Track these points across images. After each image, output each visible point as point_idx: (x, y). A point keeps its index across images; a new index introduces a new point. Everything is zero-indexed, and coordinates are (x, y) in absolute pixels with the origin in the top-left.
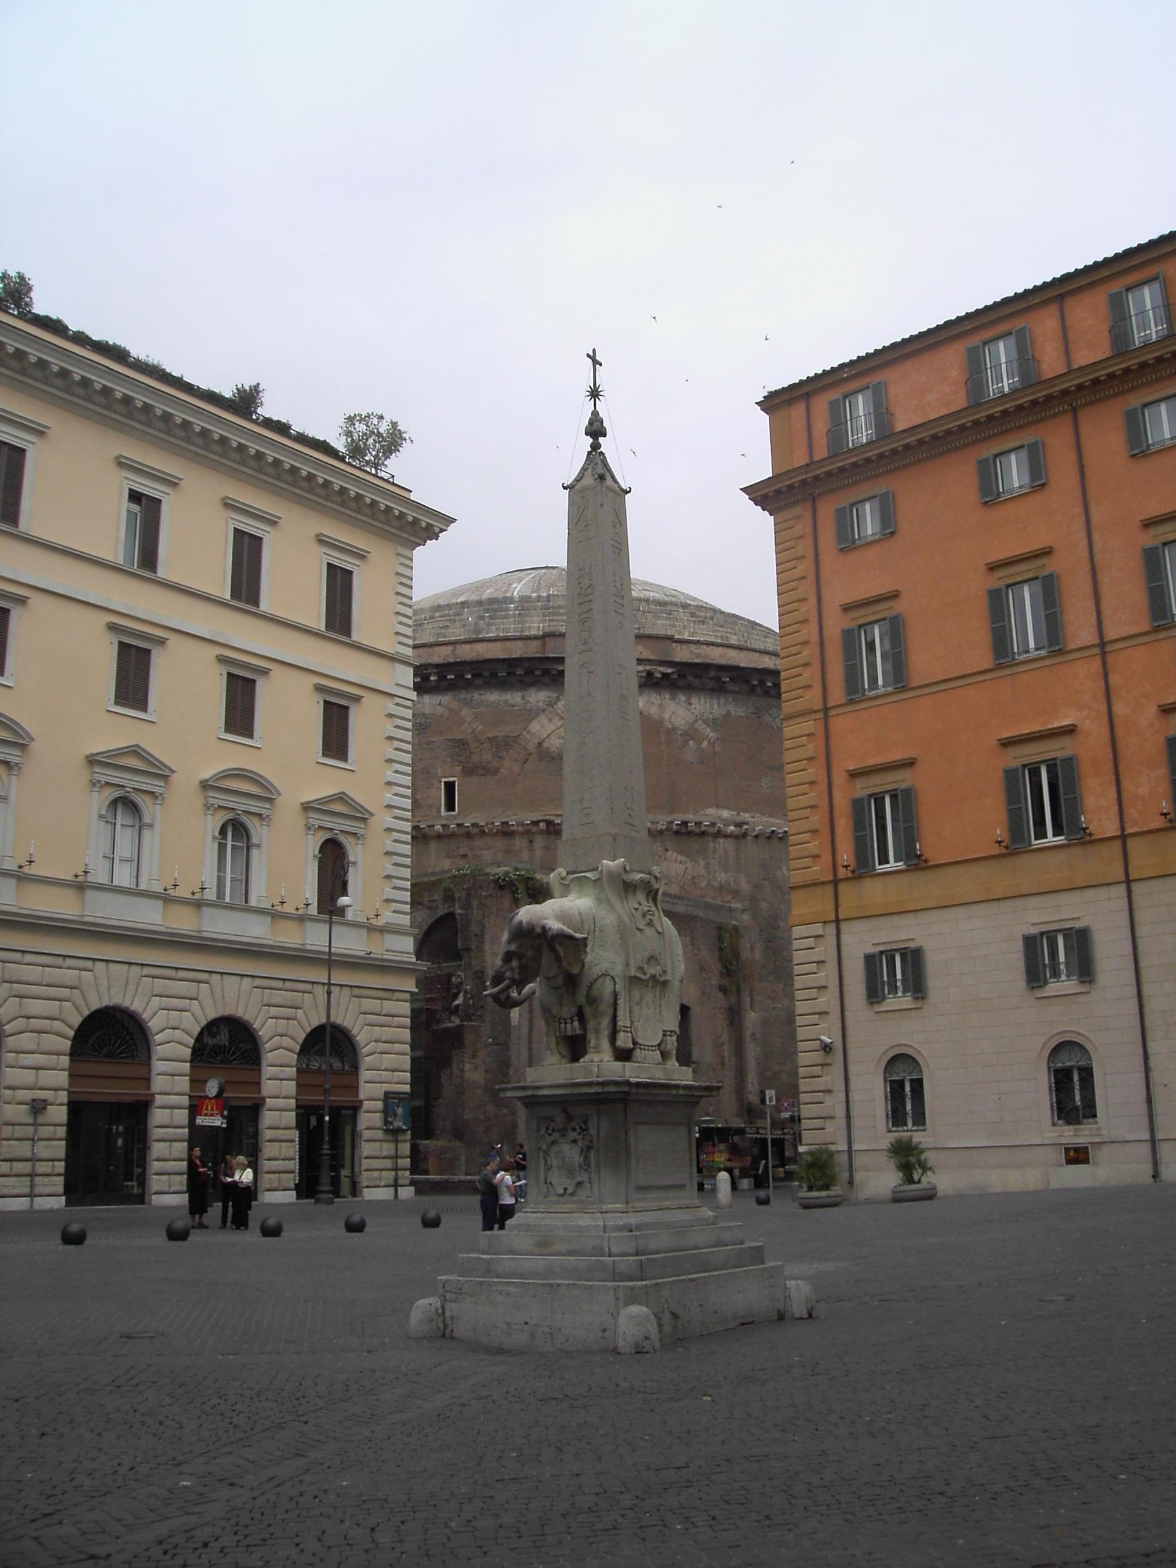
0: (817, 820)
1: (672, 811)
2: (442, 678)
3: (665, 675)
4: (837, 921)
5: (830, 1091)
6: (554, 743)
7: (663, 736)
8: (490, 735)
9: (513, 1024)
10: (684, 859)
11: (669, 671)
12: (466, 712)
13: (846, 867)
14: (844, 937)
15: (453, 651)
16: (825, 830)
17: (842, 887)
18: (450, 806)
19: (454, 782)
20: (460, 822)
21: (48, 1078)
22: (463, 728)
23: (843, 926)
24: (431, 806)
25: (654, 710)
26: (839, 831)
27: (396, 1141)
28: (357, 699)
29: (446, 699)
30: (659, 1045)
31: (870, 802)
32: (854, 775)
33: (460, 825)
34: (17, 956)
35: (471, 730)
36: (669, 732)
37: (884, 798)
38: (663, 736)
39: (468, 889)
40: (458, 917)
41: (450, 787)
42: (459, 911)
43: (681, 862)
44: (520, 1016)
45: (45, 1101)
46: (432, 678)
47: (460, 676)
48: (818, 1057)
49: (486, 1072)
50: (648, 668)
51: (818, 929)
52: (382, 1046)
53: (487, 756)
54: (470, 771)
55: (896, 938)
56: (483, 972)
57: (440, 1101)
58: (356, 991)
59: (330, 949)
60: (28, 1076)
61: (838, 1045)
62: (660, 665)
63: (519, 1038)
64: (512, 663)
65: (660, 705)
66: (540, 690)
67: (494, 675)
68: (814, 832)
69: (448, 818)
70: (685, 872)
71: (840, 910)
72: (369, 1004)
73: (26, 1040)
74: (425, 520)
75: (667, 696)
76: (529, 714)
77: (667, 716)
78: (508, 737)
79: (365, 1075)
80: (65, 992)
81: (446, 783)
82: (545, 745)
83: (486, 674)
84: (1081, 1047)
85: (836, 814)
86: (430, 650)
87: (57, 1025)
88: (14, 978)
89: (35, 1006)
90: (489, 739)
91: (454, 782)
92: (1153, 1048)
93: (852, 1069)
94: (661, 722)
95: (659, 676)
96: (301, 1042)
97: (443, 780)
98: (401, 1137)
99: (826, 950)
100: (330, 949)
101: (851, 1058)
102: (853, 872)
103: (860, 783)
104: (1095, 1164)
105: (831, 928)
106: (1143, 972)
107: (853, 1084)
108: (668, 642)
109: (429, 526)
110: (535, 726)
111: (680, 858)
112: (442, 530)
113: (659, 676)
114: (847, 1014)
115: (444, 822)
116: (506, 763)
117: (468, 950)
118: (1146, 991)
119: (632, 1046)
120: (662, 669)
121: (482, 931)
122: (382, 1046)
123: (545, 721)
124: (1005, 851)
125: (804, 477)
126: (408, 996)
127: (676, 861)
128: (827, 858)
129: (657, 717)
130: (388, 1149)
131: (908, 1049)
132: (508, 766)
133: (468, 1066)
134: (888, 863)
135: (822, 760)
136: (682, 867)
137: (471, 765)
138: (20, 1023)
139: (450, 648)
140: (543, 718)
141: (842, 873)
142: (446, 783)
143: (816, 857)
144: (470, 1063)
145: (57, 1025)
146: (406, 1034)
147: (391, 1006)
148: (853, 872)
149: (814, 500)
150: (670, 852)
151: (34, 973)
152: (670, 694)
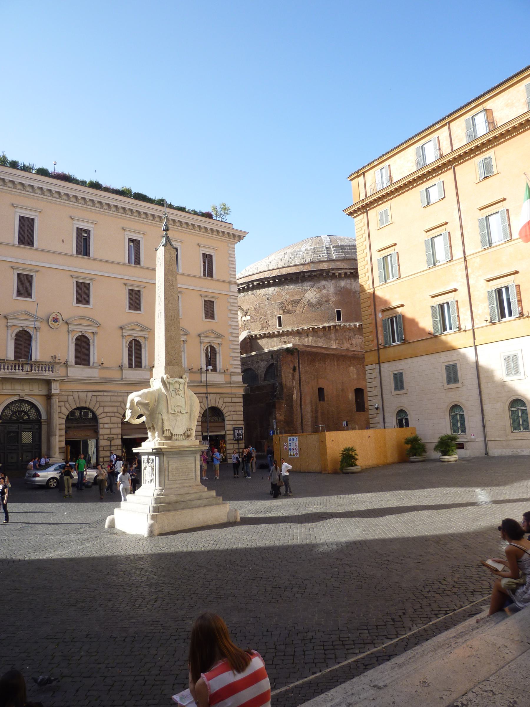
0: (372, 328)
1: (356, 321)
2: (274, 281)
3: (351, 273)
4: (379, 363)
5: (379, 423)
6: (314, 301)
7: (352, 295)
8: (291, 300)
9: (294, 399)
10: (361, 337)
11: (353, 271)
12: (283, 293)
13: (381, 344)
14: (382, 369)
15: (279, 271)
16: (374, 331)
17: (381, 351)
18: (280, 325)
19: (280, 317)
20: (283, 330)
21: (114, 431)
22: (282, 298)
23: (382, 365)
24: (274, 325)
25: (348, 286)
26: (379, 332)
27: (239, 444)
28: (217, 298)
29: (277, 288)
30: (184, 434)
31: (388, 321)
32: (383, 311)
33: (283, 331)
34: (101, 394)
35: (285, 298)
36: (354, 293)
37: (393, 319)
38: (352, 295)
39: (277, 355)
40: (274, 364)
41: (279, 318)
42: (275, 362)
43: (360, 338)
44: (297, 397)
45: (113, 437)
46: (271, 282)
47: (280, 280)
48: (375, 411)
49: (284, 416)
50: (345, 271)
51: (373, 366)
52: (232, 413)
53: (291, 307)
54: (284, 313)
55: (398, 369)
56: (282, 383)
57: (270, 426)
58: (221, 395)
59: (207, 384)
60: (107, 431)
61: (381, 406)
62: (349, 270)
63: (297, 404)
64: (297, 274)
65: (350, 284)
66: (308, 282)
67: (292, 279)
68: (371, 332)
69: (280, 329)
70: (362, 342)
71: (380, 359)
72: (227, 400)
73: (106, 420)
74: (237, 234)
75: (353, 280)
76: (304, 292)
77: (353, 287)
78: (297, 299)
79: (227, 423)
80: (118, 404)
81: (278, 317)
82: (311, 301)
83: (289, 279)
84: (460, 407)
85: (378, 325)
86: (272, 271)
87: (117, 414)
88: (100, 401)
89: (107, 409)
90: (291, 301)
91: (281, 317)
92: (485, 407)
93: (386, 415)
94: (351, 290)
95: (349, 273)
96: (202, 413)
97: (277, 316)
98: (240, 442)
99: (376, 374)
100: (207, 384)
101: (385, 411)
102: (384, 346)
103: (385, 313)
104: (466, 449)
105: (377, 366)
106: (481, 379)
107: (386, 420)
108: (354, 261)
109: (239, 236)
110: (306, 295)
111: (360, 337)
112: (244, 237)
113: (349, 273)
114: (384, 396)
115: (278, 330)
116: (298, 308)
117: (277, 375)
118: (482, 386)
119: (170, 435)
120: (350, 271)
121: (281, 369)
122: (232, 413)
123: (310, 293)
124: (433, 336)
125: (362, 204)
126: (241, 396)
127: (359, 338)
128: (375, 341)
129: (349, 288)
130: (236, 446)
131: (403, 408)
132: (298, 309)
133: (277, 415)
134: (395, 342)
135: (373, 307)
136: (361, 340)
137: (286, 310)
138: (104, 415)
139: (278, 270)
140: (309, 292)
141: (381, 347)
142: (278, 317)
143: (372, 341)
144: (278, 414)
145: (117, 414)
146: (241, 409)
147: (235, 400)
148: (384, 346)
149: (367, 212)
150: (356, 335)
151: (108, 399)
152: (354, 279)
